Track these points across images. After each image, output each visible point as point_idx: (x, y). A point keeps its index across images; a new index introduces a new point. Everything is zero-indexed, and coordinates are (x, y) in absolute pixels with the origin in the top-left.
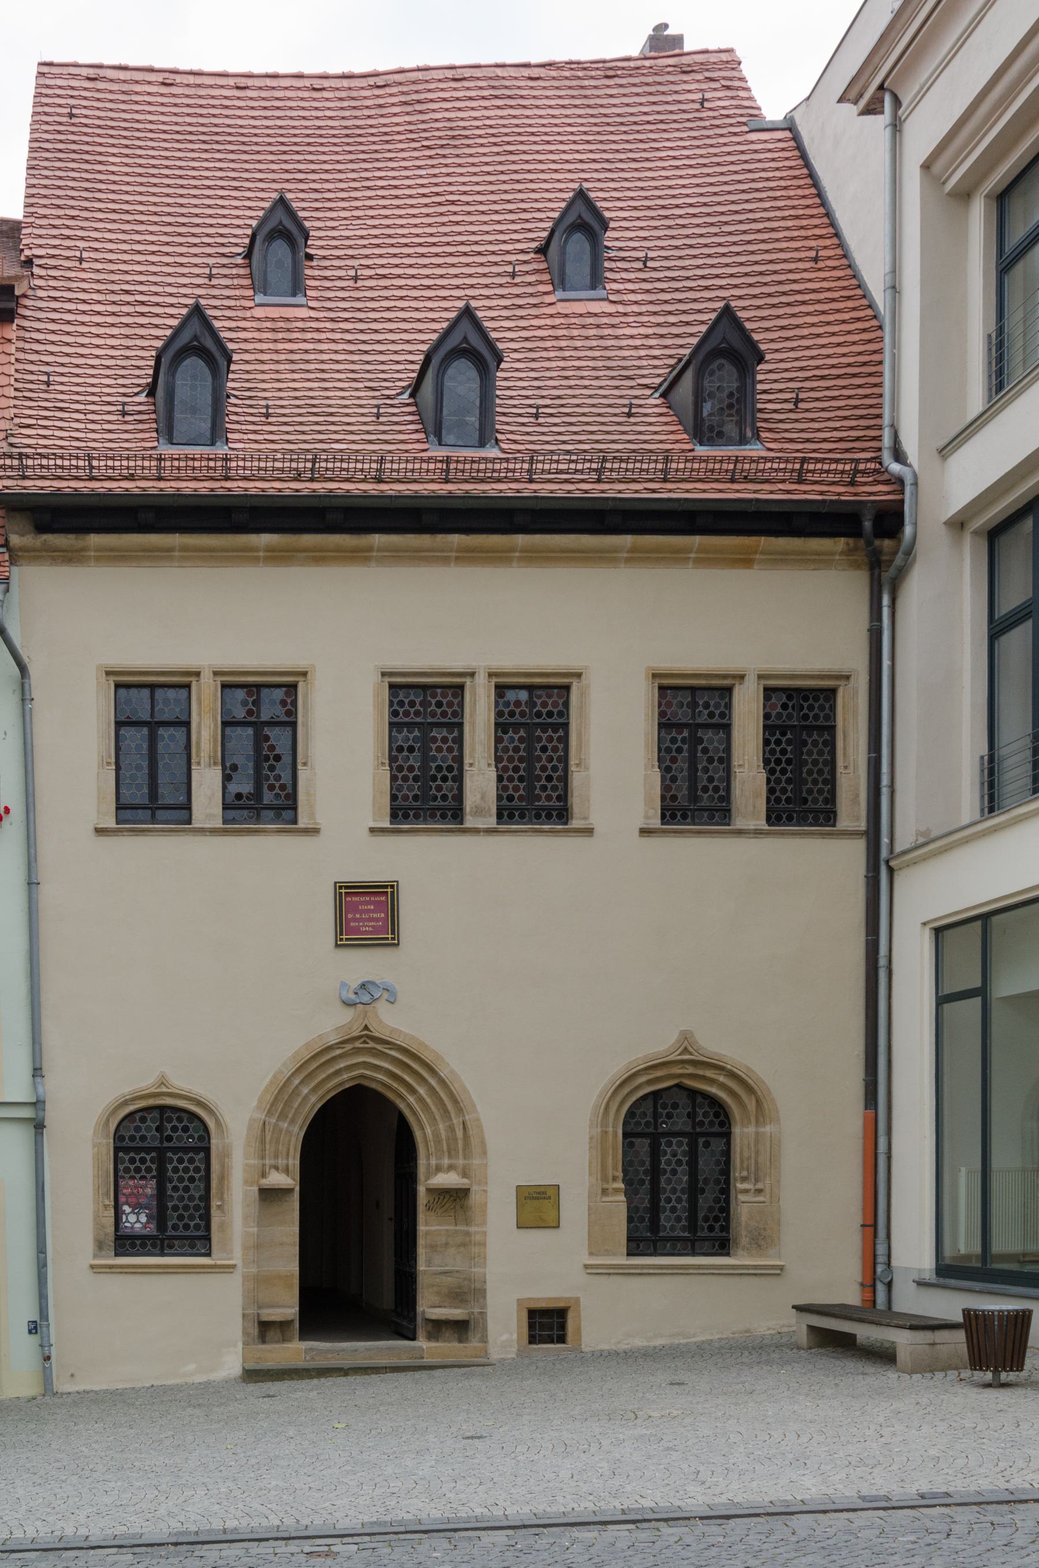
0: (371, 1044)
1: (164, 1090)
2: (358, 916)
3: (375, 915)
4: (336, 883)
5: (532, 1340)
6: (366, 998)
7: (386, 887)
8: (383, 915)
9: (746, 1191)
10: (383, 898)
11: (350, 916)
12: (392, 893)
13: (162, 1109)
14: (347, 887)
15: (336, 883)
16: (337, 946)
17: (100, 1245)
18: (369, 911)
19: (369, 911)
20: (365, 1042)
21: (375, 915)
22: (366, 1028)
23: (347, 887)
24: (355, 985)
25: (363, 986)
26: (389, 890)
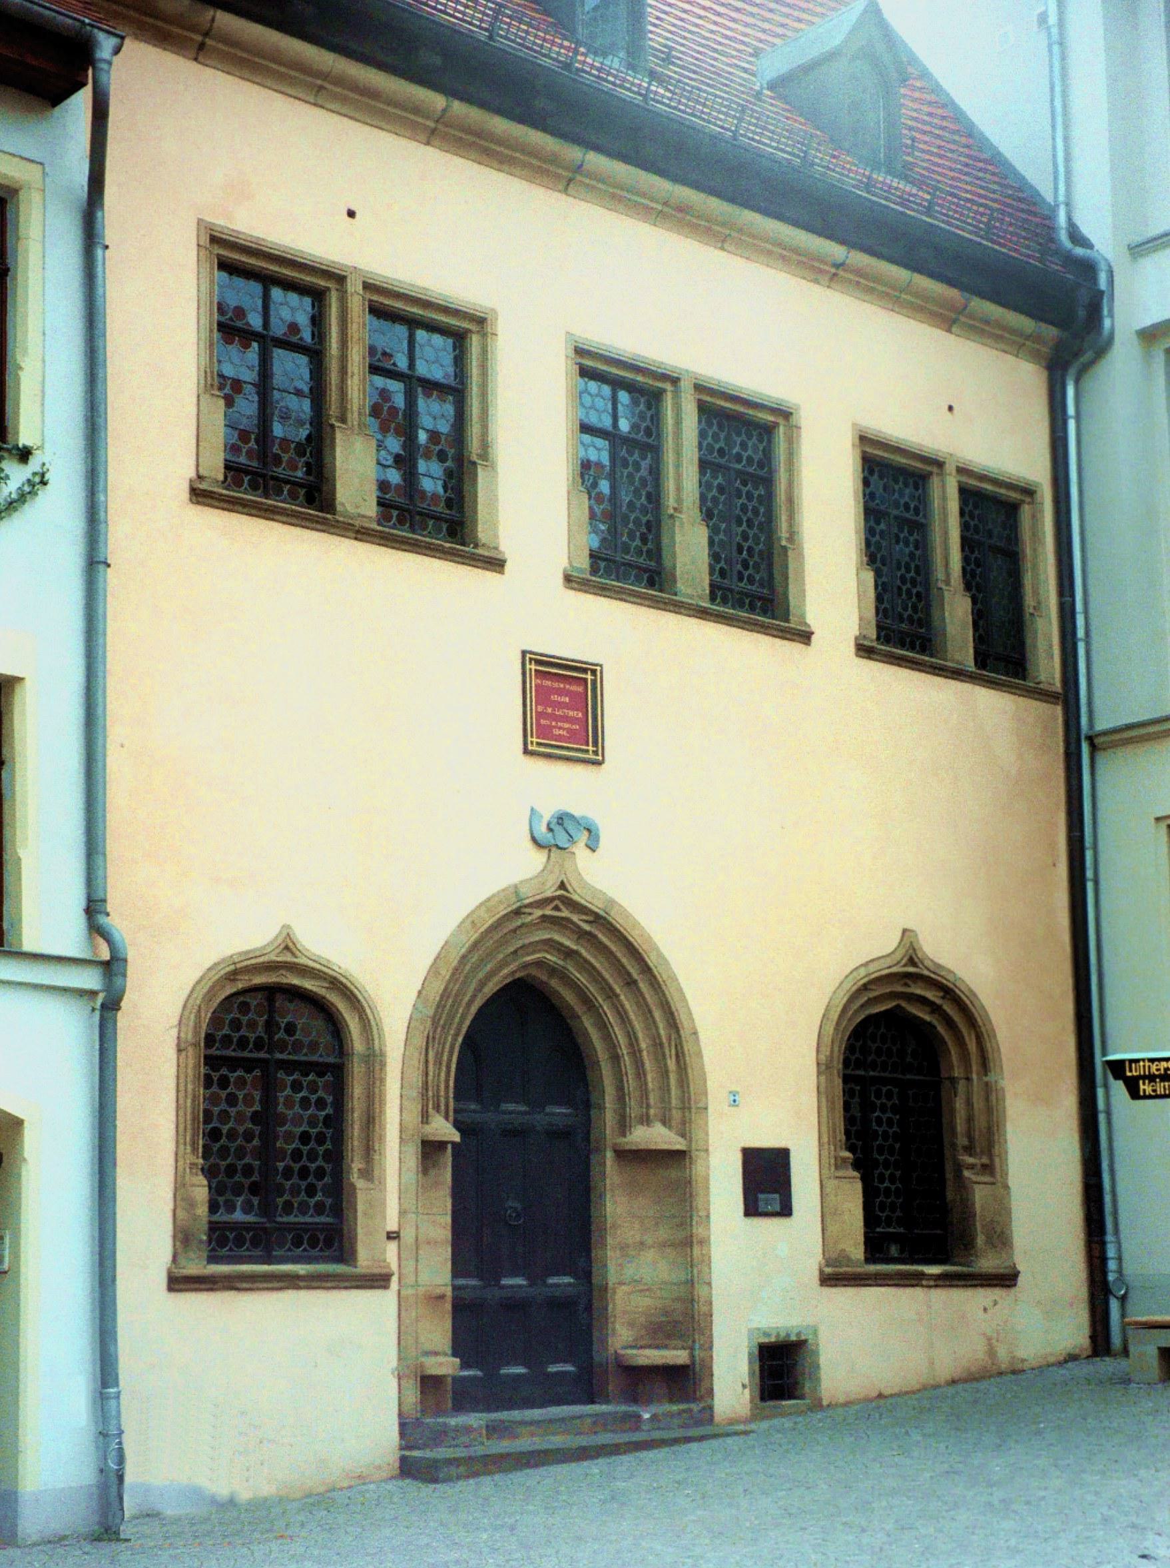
0: (565, 913)
1: (288, 958)
2: (549, 710)
3: (571, 713)
4: (524, 653)
5: (763, 1399)
6: (562, 839)
7: (585, 671)
8: (580, 715)
9: (972, 1167)
10: (580, 689)
11: (540, 709)
12: (594, 682)
13: (272, 992)
14: (539, 662)
15: (524, 653)
16: (526, 751)
17: (183, 1238)
18: (560, 705)
19: (560, 705)
20: (557, 908)
21: (571, 713)
22: (562, 886)
23: (539, 662)
24: (547, 817)
25: (562, 819)
26: (589, 677)
